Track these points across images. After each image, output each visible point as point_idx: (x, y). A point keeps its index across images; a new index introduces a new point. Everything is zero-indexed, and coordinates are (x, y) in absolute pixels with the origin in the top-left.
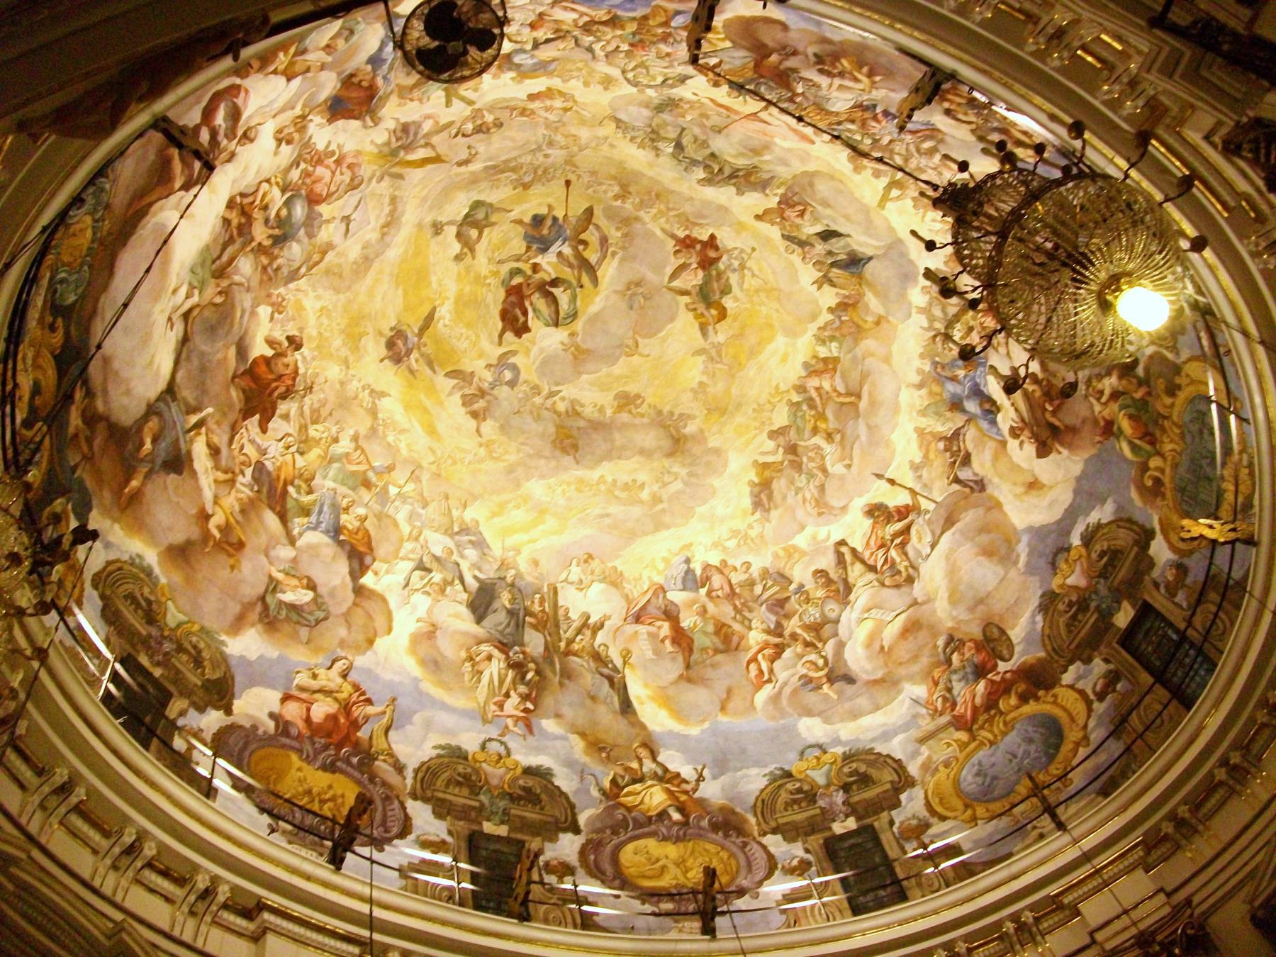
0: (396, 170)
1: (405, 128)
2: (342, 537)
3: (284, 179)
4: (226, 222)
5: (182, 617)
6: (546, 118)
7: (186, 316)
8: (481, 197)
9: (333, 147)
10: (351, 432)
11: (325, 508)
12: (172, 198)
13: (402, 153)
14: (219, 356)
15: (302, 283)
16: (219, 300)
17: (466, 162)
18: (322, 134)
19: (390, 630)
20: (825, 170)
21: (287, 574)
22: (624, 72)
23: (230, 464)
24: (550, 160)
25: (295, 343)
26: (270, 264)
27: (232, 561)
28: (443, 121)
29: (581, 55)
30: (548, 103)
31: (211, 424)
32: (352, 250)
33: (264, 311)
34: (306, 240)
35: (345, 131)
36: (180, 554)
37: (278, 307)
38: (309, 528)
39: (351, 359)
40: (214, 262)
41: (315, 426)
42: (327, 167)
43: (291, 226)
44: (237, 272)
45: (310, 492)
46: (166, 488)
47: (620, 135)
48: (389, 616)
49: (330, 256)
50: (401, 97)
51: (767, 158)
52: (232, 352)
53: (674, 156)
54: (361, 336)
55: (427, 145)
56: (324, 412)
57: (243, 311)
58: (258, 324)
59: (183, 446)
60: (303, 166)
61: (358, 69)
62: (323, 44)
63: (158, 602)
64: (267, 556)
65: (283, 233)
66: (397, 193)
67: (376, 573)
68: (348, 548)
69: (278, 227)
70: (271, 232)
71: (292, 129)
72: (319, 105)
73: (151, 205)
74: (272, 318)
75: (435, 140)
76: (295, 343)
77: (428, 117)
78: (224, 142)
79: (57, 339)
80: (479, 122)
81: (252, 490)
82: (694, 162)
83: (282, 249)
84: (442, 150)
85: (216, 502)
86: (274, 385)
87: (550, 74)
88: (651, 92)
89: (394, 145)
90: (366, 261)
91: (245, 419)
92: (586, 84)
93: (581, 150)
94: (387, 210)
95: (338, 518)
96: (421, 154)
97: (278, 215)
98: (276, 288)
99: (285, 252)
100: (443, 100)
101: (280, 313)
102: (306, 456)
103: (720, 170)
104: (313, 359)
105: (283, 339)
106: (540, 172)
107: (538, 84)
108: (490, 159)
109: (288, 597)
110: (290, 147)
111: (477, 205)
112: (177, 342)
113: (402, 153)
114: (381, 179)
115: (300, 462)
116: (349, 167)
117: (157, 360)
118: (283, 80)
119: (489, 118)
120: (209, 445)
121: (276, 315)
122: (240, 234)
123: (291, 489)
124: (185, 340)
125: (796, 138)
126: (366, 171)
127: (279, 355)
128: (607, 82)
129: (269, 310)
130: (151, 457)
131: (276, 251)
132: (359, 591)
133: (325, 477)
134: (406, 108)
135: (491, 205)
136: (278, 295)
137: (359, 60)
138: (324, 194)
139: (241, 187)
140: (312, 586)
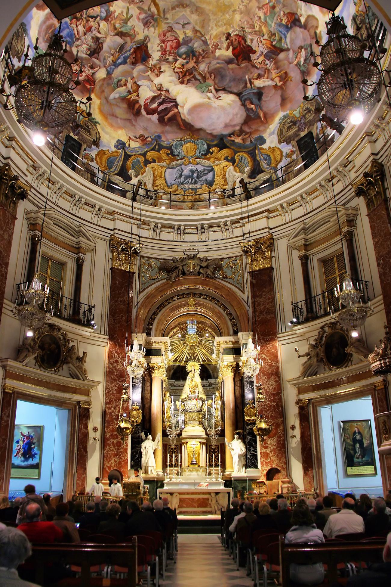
0: (162, 15)
1: (146, 24)
2: (289, 26)
4: (188, 83)
5: (298, 110)
7: (217, 91)
9: (159, 48)
10: (257, 10)
11: (280, 29)
12: (180, 111)
13: (155, 17)
14: (231, 72)
15: (207, 38)
16: (213, 77)
18: (155, 55)
19: (317, 19)
21: (296, 57)
23: (263, 69)
25: (228, 36)
27: (290, 80)
28: (138, 11)
31: (251, 77)
32: (194, 18)
33: (218, 53)
34: (193, 41)
35: (152, 48)
36: (284, 101)
37: (216, 47)
38: (285, 40)
39: (233, 9)
40: (201, 83)
42: (166, 46)
43: (188, 51)
44: (204, 71)
45: (274, 34)
46: (265, 101)
48: (313, 16)
49: (197, 28)
52: (230, 66)
54: (225, 5)
55: (149, 9)
56: (251, 23)
57: (218, 63)
58: (222, 55)
59: (256, 91)
60: (167, 57)
62: (124, 87)
63: (292, 117)
64: (290, 63)
65: (192, 54)
67: (301, 15)
68: (292, 24)
71: (156, 70)
72: (146, 66)
73: (182, 119)
74: (220, 49)
75: (146, 8)
76: (228, 36)
77: (138, 19)
78: (163, 97)
79: (215, 149)
81: (272, 62)
83: (196, 52)
85: (272, 80)
94: (177, 9)
95: (284, 25)
96: (154, 9)
100: (131, 20)
102: (265, 33)
104: (233, 27)
105: (227, 42)
109: (302, 60)
112: (225, 93)
114: (167, 19)
115: (266, 37)
116: (165, 36)
117: (230, 102)
118: (140, 89)
120: (257, 79)
121: (219, 47)
122: (192, 73)
123: (274, 43)
124: (224, 90)
126: (164, 27)
127: (232, 45)
129: (217, 51)
130: (257, 106)
132: (305, 27)
133: (271, 26)
136: (212, 48)
138: (175, 41)
139: (176, 80)
140: (301, 48)
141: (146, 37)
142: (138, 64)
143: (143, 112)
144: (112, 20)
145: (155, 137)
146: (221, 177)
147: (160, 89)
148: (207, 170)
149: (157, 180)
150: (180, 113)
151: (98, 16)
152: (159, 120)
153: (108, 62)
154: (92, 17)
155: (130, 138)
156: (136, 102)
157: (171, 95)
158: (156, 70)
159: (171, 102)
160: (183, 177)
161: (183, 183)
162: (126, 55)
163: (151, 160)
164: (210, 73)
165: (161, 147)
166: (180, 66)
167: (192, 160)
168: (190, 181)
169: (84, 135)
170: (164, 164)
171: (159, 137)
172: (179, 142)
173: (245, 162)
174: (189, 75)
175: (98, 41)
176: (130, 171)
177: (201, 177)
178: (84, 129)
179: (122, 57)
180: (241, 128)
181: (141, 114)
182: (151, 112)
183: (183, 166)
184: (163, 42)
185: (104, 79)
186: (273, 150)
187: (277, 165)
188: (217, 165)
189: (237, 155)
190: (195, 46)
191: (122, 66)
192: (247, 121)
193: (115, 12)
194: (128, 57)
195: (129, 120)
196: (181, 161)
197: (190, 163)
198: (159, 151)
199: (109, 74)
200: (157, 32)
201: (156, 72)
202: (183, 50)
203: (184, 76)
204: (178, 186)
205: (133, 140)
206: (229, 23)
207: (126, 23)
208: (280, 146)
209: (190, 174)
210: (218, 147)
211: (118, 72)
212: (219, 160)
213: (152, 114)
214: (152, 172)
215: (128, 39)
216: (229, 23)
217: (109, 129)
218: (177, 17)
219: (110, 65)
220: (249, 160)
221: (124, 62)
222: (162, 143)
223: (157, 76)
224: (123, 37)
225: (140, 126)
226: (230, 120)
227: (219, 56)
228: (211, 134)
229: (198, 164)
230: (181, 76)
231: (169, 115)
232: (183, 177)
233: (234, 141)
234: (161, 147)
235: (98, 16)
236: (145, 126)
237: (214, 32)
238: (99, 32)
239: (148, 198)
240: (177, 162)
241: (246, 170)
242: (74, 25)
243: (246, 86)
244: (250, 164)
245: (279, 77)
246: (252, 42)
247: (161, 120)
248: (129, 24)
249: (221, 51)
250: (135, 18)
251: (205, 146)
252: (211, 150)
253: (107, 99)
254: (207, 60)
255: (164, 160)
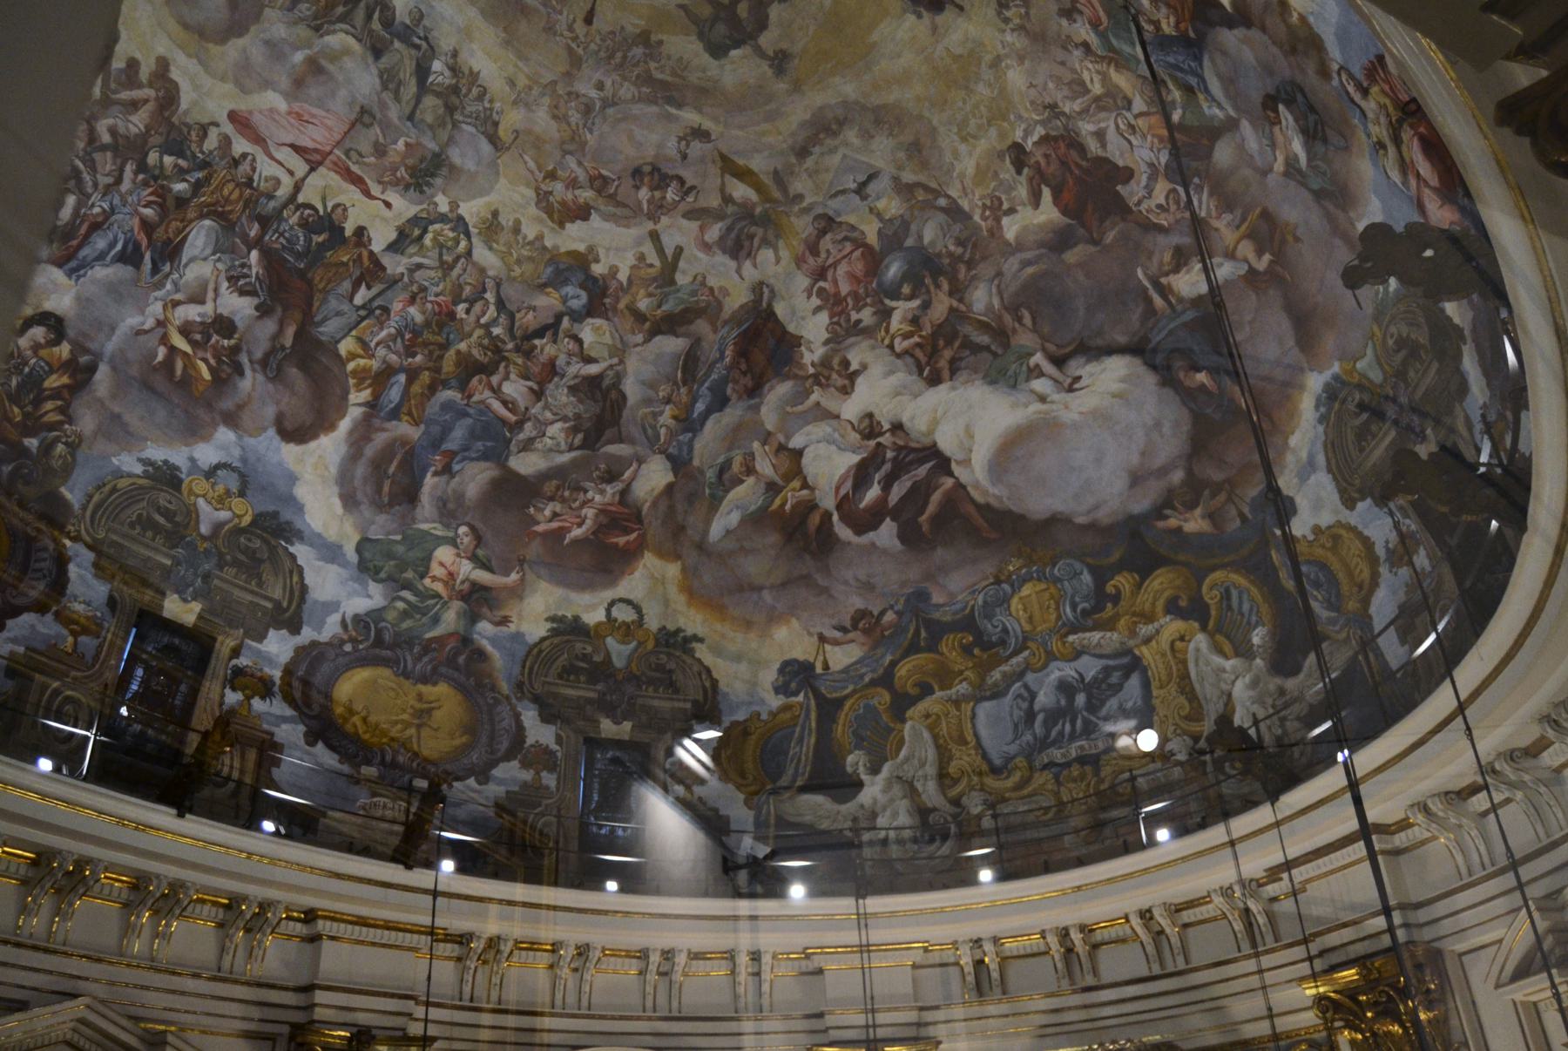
0: (777, 194)
1: (738, 248)
3: (877, 326)
4: (953, 372)
6: (580, 164)
7: (1059, 362)
8: (706, 58)
9: (815, 301)
13: (758, 210)
14: (1081, 278)
15: (954, 193)
16: (1027, 320)
17: (701, 134)
18: (813, 328)
20: (214, 49)
22: (469, 253)
24: (598, 76)
25: (1018, 155)
26: (960, 258)
28: (694, 226)
29: (509, 291)
30: (570, 196)
31: (1154, 269)
32: (881, 153)
33: (1011, 228)
34: (913, 227)
35: (794, 313)
37: (997, 210)
39: (988, 58)
40: (995, 355)
41: (1089, 85)
42: (835, 282)
44: (989, 308)
47: (497, 105)
49: (908, 177)
50: (720, 305)
51: (299, 57)
52: (1071, 257)
53: (432, 52)
54: (957, 58)
55: (727, 199)
57: (1026, 264)
58: (1025, 228)
59: (1189, 315)
60: (854, 316)
61: (740, 398)
62: (751, 481)
66: (793, 160)
69: (923, 283)
70: (932, 288)
71: (835, 376)
72: (796, 377)
74: (1012, 211)
75: (714, 202)
76: (1018, 155)
77: (706, 247)
78: (890, 454)
79: (1122, 582)
80: (657, 194)
82: (405, 35)
83: (939, 255)
84: (713, 179)
86: (1077, 172)
87: (553, 258)
88: (444, 207)
89: (760, 232)
90: (882, 118)
91: (1130, 211)
92: (517, 230)
93: (554, 83)
94: (817, 150)
96: (740, 191)
97: (910, 298)
98: (978, 228)
99: (939, 247)
100: (682, 264)
101: (1001, 203)
103: (369, 17)
104: (1020, 117)
105: (1023, 179)
106: (619, 55)
107: (574, 237)
108: (670, 118)
110: (850, 357)
111: (718, 51)
112: (1089, 361)
113: (758, 210)
114: (799, 197)
117: (1116, 387)
118: (805, 461)
119: (644, 194)
121: (1005, 206)
122: (955, 335)
125: (259, 121)
126: (803, 226)
128: (492, 226)
129: (1005, 221)
130: (1213, 371)
131: (946, 261)
134: (722, 284)
135: (701, 36)
136: (985, 219)
137: (732, 414)
138: (858, 253)
141: (758, 288)
142: (767, 387)
143: (843, 532)
144: (617, 300)
145: (907, 601)
146: (1173, 688)
147: (869, 427)
148: (1115, 668)
149: (950, 758)
150: (964, 487)
151: (558, 318)
152: (903, 537)
153: (663, 431)
154: (540, 333)
155: (822, 639)
156: (811, 506)
157: (913, 435)
158: (835, 376)
159: (922, 462)
160: (1040, 717)
161: (1043, 744)
162: (714, 376)
163: (913, 691)
164: (1014, 309)
165: (937, 631)
166: (907, 328)
167: (1055, 645)
168: (1068, 727)
169: (656, 703)
170: (962, 688)
171: (922, 596)
172: (992, 590)
173: (1246, 607)
174: (949, 343)
175: (599, 386)
176: (850, 759)
177: (1103, 703)
178: (651, 682)
179: (704, 390)
180: (1190, 472)
181: (838, 539)
182: (865, 522)
183: (1030, 678)
184: (821, 274)
185: (670, 489)
186: (1331, 536)
187: (1366, 602)
188: (1147, 641)
189: (1208, 581)
190: (926, 240)
191: (713, 417)
192: (1201, 441)
193: (614, 271)
194: (724, 381)
195: (806, 580)
196: (1019, 658)
197: (1051, 657)
198: (932, 647)
199: (679, 464)
200: (784, 254)
201: (840, 382)
202: (894, 269)
203: (933, 353)
204: (1029, 758)
205: (836, 643)
206: (1000, 111)
207: (672, 282)
208: (1352, 518)
209: (1063, 702)
210: (1131, 571)
211: (707, 444)
212: (1149, 618)
213: (875, 526)
214: (926, 735)
215: (701, 326)
216: (1000, 111)
217: (737, 640)
218: (828, 177)
219: (672, 434)
220: (1254, 591)
221: (720, 402)
222: (936, 615)
223: (846, 391)
224: (682, 330)
225: (846, 583)
226: (1143, 454)
227: (1017, 238)
228: (1092, 527)
229: (1077, 654)
230: (923, 359)
231: (931, 508)
232: (1040, 718)
233: (1178, 530)
234: (937, 631)
235: (558, 318)
236: (863, 577)
237: (968, 166)
238: (589, 360)
239: (932, 840)
240: (1005, 668)
241: (1256, 640)
242: (482, 395)
243: (1150, 310)
244: (1265, 609)
245: (1250, 235)
246: (1104, 145)
247: (910, 536)
248: (682, 279)
249: (1017, 217)
250: (692, 250)
251: (1087, 577)
252: (1110, 589)
253: (701, 547)
254: (987, 270)
255: (961, 672)
